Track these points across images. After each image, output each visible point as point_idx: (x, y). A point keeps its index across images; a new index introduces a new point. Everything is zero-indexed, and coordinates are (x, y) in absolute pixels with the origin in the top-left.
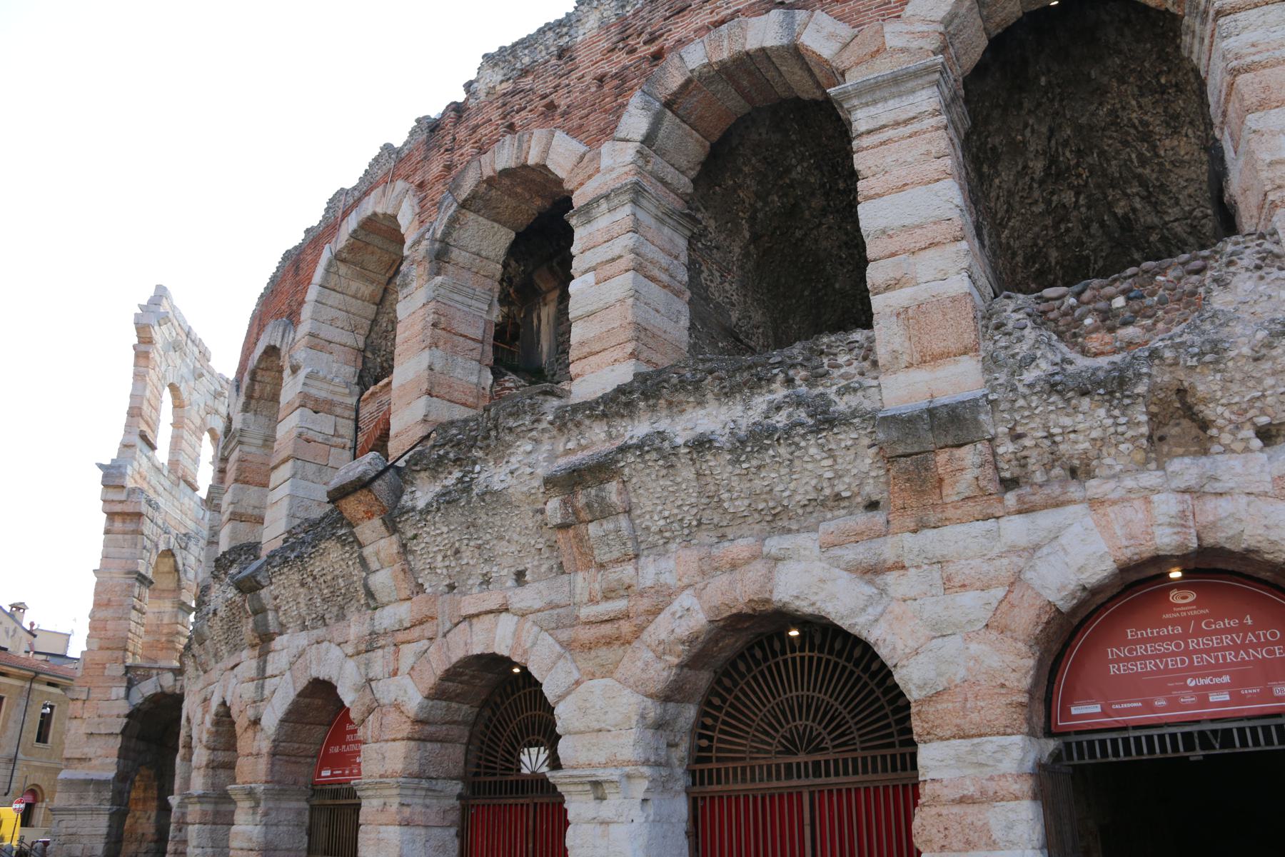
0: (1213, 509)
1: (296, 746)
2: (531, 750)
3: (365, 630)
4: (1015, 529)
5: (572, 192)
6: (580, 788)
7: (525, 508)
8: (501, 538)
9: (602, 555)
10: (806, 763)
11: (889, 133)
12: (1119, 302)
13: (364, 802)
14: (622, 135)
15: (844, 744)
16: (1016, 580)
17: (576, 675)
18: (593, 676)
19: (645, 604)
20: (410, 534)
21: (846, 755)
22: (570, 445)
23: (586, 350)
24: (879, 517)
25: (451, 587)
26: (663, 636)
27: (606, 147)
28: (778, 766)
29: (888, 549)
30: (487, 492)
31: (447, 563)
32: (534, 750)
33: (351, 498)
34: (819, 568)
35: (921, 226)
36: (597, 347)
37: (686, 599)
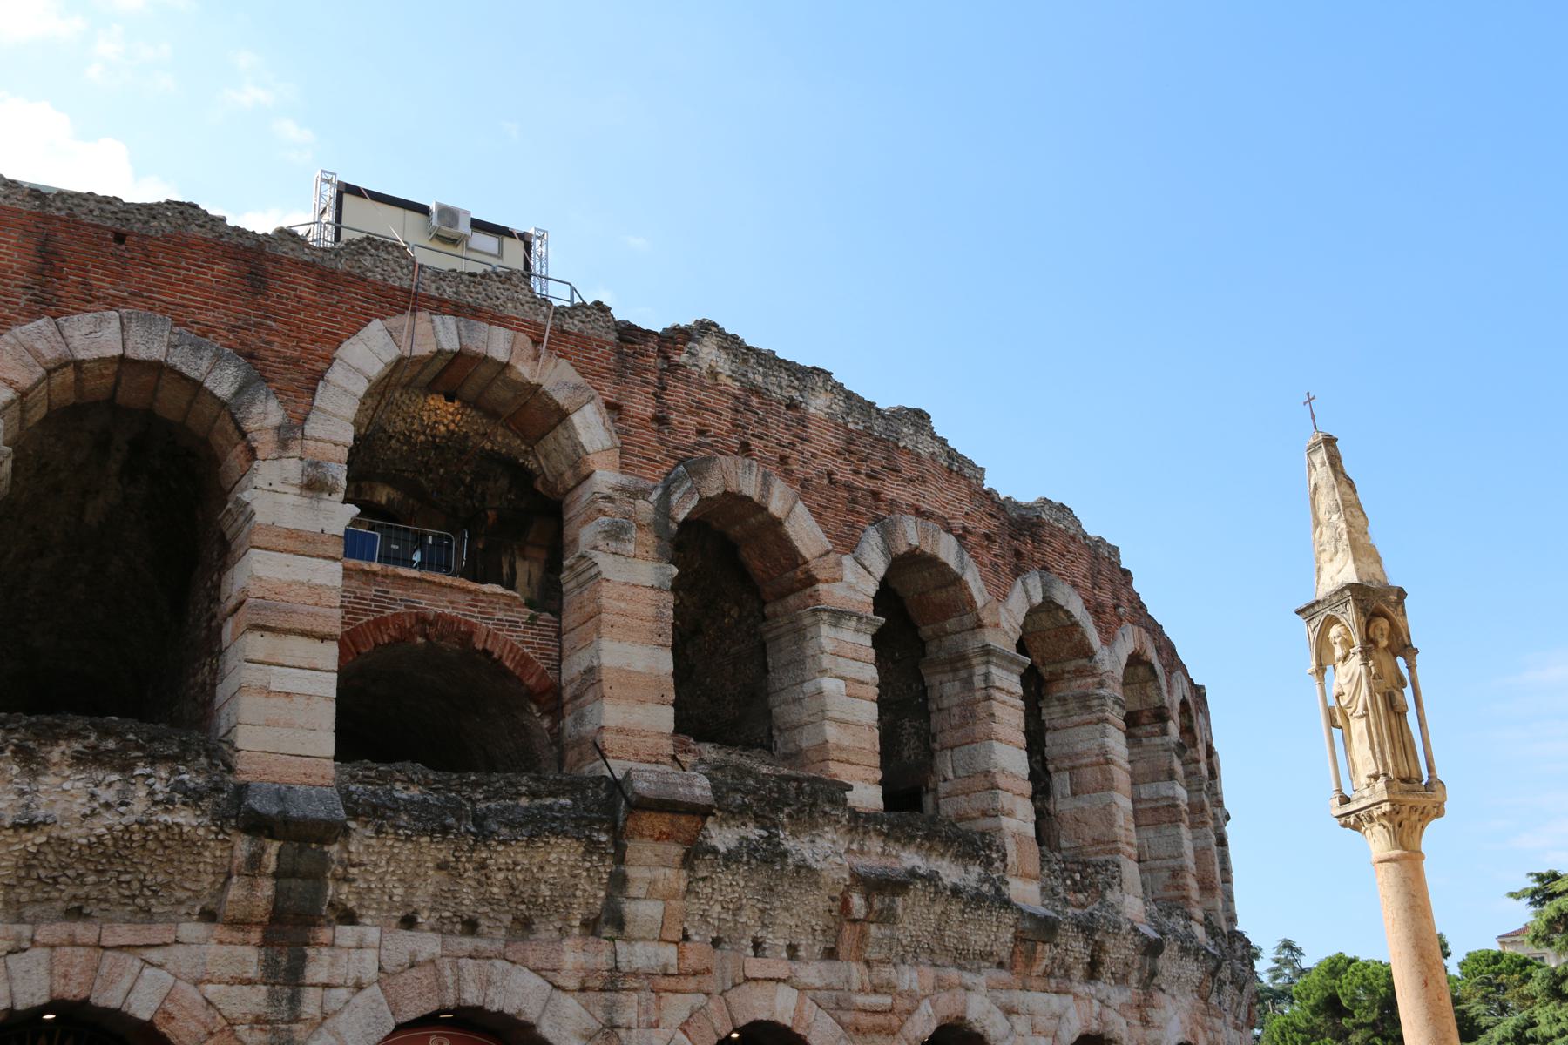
3: (602, 960)
5: (818, 581)
7: (826, 891)
8: (787, 910)
9: (872, 953)
12: (1078, 877)
14: (867, 563)
20: (702, 873)
22: (855, 847)
23: (844, 756)
25: (716, 943)
30: (802, 868)
33: (668, 816)
37: (926, 1007)
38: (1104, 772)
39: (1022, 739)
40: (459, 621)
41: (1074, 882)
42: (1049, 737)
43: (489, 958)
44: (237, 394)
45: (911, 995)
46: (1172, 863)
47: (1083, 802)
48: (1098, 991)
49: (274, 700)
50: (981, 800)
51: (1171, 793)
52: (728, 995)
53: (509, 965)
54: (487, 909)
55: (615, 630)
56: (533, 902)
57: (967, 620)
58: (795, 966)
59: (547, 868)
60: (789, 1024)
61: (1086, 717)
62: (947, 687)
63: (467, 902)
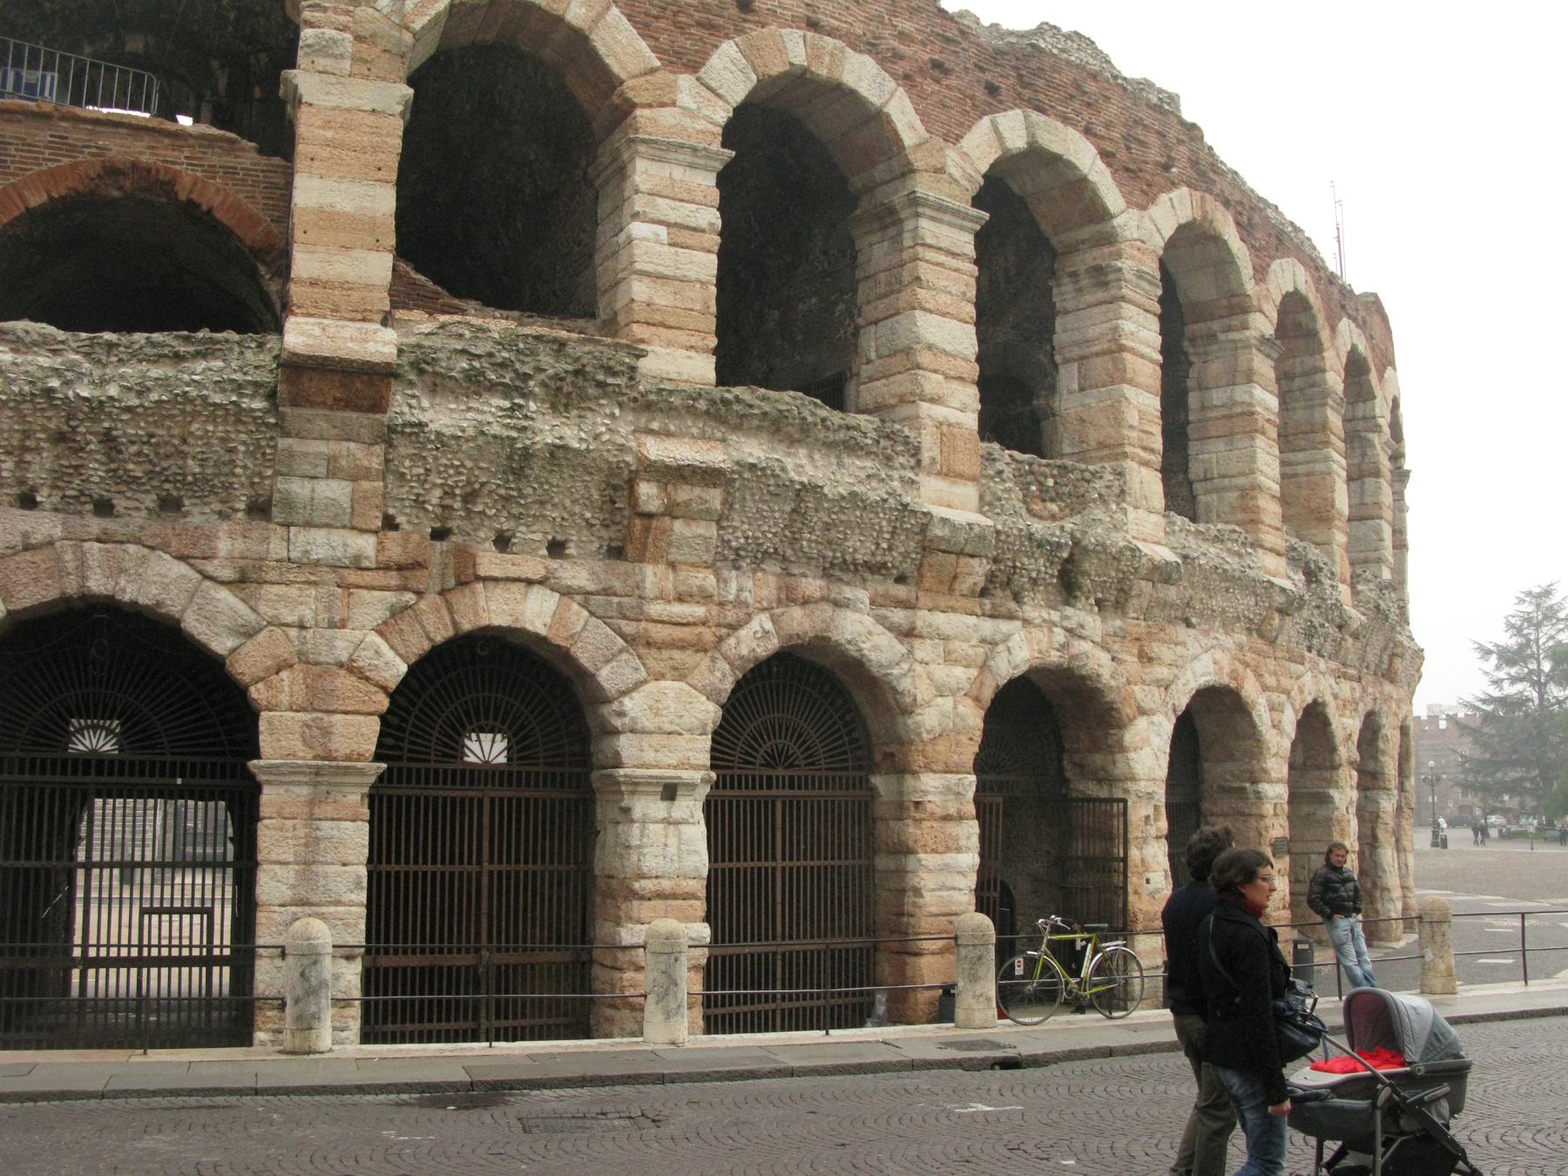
2: (482, 736)
4: (988, 627)
5: (634, 106)
9: (674, 555)
12: (1051, 482)
13: (266, 789)
14: (713, 84)
15: (812, 764)
16: (984, 667)
17: (643, 674)
18: (660, 676)
19: (731, 615)
22: (655, 425)
23: (658, 317)
26: (745, 652)
27: (685, 81)
28: (761, 777)
31: (448, 502)
32: (486, 738)
34: (869, 621)
35: (954, 357)
36: (671, 321)
37: (762, 622)
38: (1115, 361)
39: (970, 310)
40: (158, 171)
42: (1059, 323)
43: (122, 542)
45: (739, 603)
46: (1241, 481)
48: (1067, 618)
50: (900, 384)
51: (1246, 398)
52: (451, 597)
53: (146, 551)
54: (123, 488)
55: (316, 163)
56: (180, 479)
58: (554, 564)
59: (190, 440)
60: (543, 632)
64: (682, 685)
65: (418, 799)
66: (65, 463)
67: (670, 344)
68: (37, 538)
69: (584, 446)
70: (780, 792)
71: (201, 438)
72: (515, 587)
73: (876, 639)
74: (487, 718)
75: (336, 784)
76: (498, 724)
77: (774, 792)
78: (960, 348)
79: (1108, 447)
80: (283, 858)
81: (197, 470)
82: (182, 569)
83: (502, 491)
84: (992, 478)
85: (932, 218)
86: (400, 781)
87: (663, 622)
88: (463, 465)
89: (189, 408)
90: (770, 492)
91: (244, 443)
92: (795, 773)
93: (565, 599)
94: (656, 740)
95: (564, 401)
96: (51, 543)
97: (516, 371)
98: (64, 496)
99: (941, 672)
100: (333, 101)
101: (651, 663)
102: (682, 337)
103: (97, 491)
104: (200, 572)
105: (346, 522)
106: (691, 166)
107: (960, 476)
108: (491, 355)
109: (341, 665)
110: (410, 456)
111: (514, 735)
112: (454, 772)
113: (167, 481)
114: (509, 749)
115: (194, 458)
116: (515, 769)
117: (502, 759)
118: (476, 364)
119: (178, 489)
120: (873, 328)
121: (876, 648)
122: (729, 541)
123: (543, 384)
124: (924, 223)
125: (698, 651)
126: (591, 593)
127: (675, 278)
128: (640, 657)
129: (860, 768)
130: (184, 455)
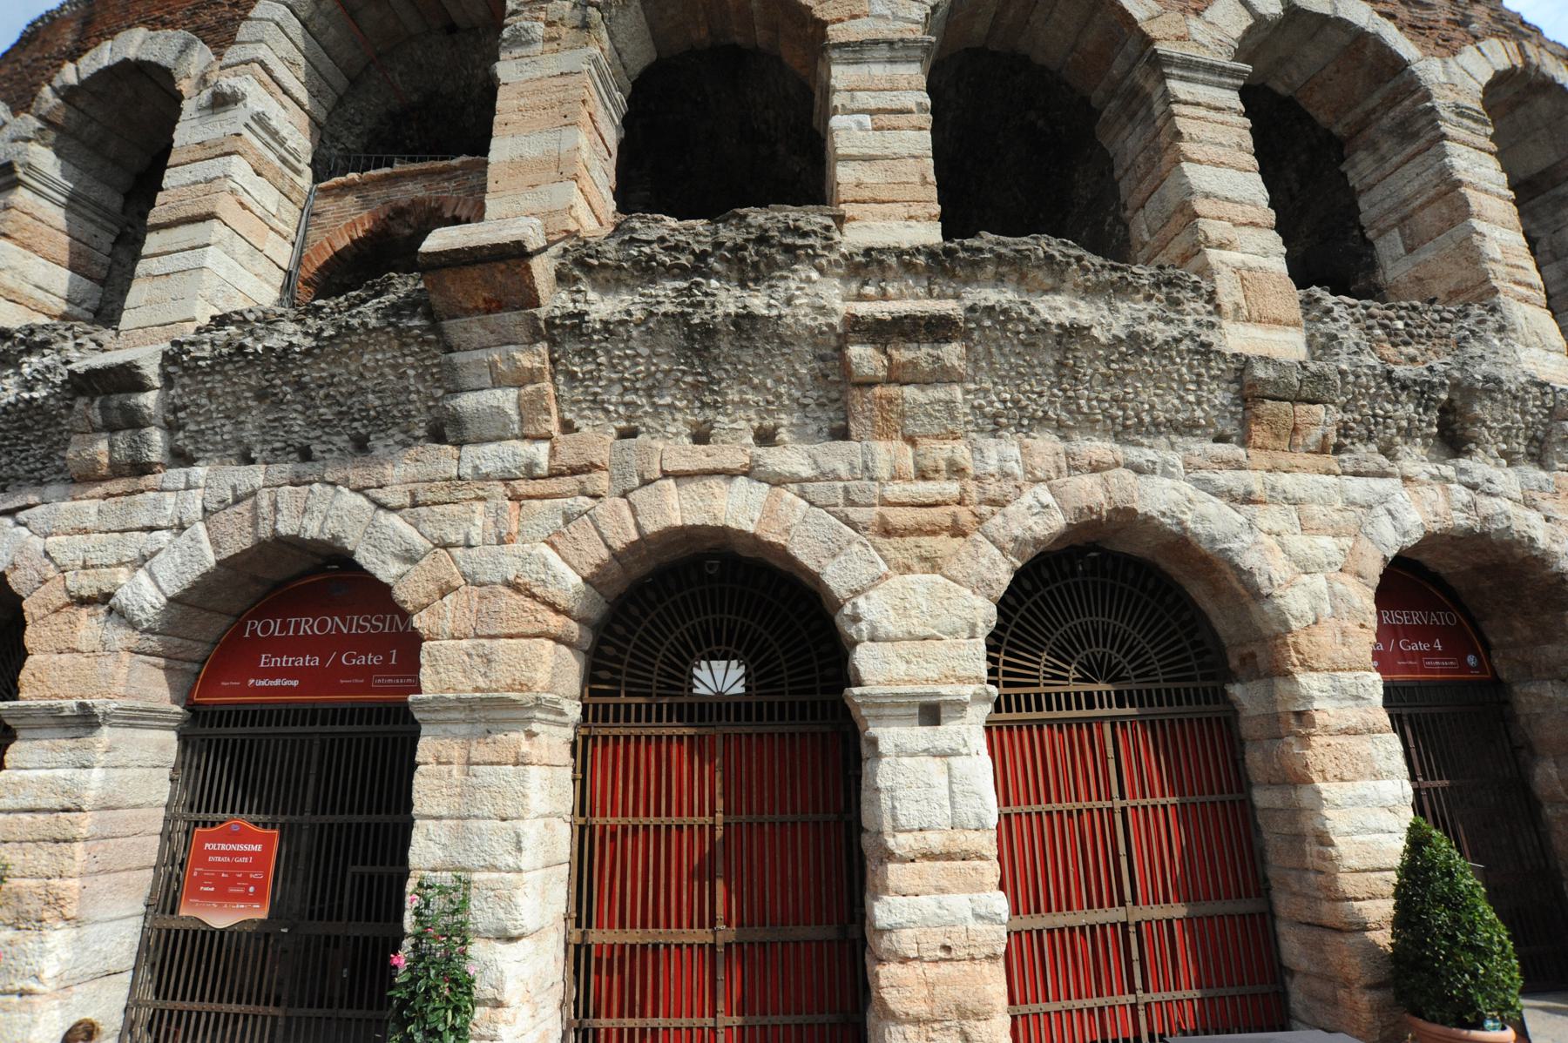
0: (1487, 505)
1: (177, 641)
4: (1358, 488)
5: (825, 24)
6: (902, 711)
9: (912, 427)
10: (1108, 693)
11: (1202, 112)
15: (1146, 674)
21: (1149, 686)
23: (866, 194)
24: (1223, 450)
26: (1018, 532)
29: (1254, 480)
32: (719, 666)
34: (1188, 488)
35: (1241, 203)
36: (884, 196)
41: (1391, 333)
42: (1363, 204)
44: (176, 59)
47: (1427, 254)
48: (1462, 471)
49: (157, 281)
52: (631, 496)
54: (318, 432)
57: (1131, 48)
59: (368, 375)
60: (751, 529)
61: (1410, 149)
62: (1130, 143)
63: (297, 429)
64: (937, 577)
65: (638, 738)
66: (270, 417)
67: (885, 217)
68: (242, 490)
69: (774, 312)
70: (1106, 712)
71: (375, 370)
72: (715, 483)
73: (1200, 508)
74: (718, 643)
75: (495, 721)
76: (732, 649)
77: (1097, 712)
78: (1247, 195)
79: (1467, 290)
80: (435, 811)
81: (377, 403)
82: (360, 500)
83: (689, 379)
84: (1320, 320)
85: (1182, 78)
86: (616, 719)
87: (903, 505)
88: (638, 355)
89: (355, 339)
90: (1022, 343)
91: (412, 367)
92: (1125, 687)
93: (777, 489)
94: (905, 647)
95: (752, 275)
96: (254, 493)
97: (693, 252)
98: (273, 450)
99: (1299, 543)
100: (528, 75)
101: (891, 554)
102: (900, 209)
103: (297, 440)
104: (374, 501)
105: (516, 431)
106: (891, 61)
107: (1277, 321)
108: (662, 240)
109: (508, 584)
110: (578, 353)
111: (752, 661)
112: (680, 705)
113: (355, 420)
114: (747, 676)
115: (374, 392)
116: (754, 699)
117: (739, 689)
118: (647, 250)
119: (364, 426)
120: (1141, 213)
121: (1203, 518)
122: (980, 407)
123: (723, 259)
124: (1175, 86)
125: (953, 536)
126: (808, 480)
127: (885, 158)
128: (878, 550)
129: (1212, 677)
130: (363, 391)
